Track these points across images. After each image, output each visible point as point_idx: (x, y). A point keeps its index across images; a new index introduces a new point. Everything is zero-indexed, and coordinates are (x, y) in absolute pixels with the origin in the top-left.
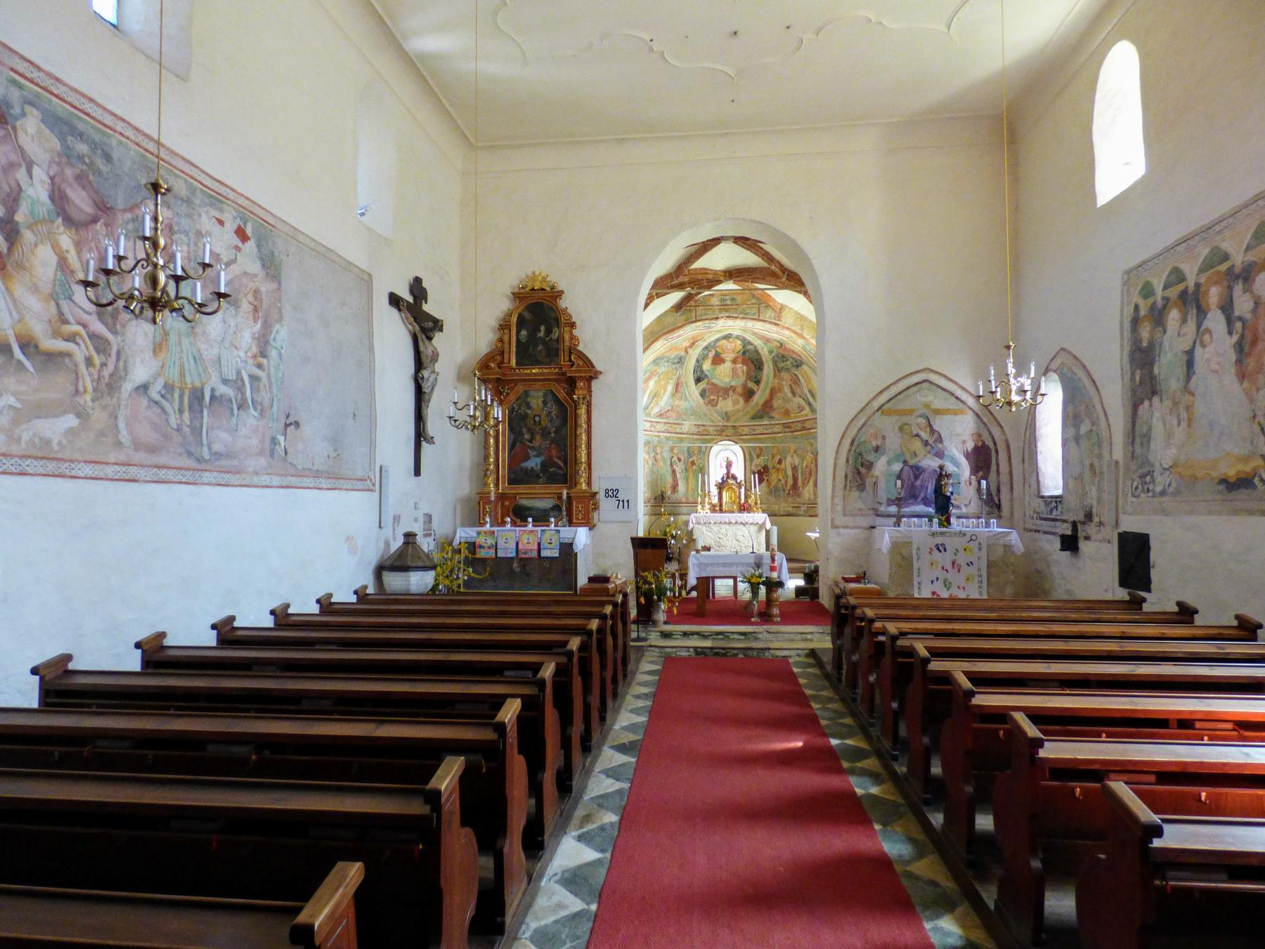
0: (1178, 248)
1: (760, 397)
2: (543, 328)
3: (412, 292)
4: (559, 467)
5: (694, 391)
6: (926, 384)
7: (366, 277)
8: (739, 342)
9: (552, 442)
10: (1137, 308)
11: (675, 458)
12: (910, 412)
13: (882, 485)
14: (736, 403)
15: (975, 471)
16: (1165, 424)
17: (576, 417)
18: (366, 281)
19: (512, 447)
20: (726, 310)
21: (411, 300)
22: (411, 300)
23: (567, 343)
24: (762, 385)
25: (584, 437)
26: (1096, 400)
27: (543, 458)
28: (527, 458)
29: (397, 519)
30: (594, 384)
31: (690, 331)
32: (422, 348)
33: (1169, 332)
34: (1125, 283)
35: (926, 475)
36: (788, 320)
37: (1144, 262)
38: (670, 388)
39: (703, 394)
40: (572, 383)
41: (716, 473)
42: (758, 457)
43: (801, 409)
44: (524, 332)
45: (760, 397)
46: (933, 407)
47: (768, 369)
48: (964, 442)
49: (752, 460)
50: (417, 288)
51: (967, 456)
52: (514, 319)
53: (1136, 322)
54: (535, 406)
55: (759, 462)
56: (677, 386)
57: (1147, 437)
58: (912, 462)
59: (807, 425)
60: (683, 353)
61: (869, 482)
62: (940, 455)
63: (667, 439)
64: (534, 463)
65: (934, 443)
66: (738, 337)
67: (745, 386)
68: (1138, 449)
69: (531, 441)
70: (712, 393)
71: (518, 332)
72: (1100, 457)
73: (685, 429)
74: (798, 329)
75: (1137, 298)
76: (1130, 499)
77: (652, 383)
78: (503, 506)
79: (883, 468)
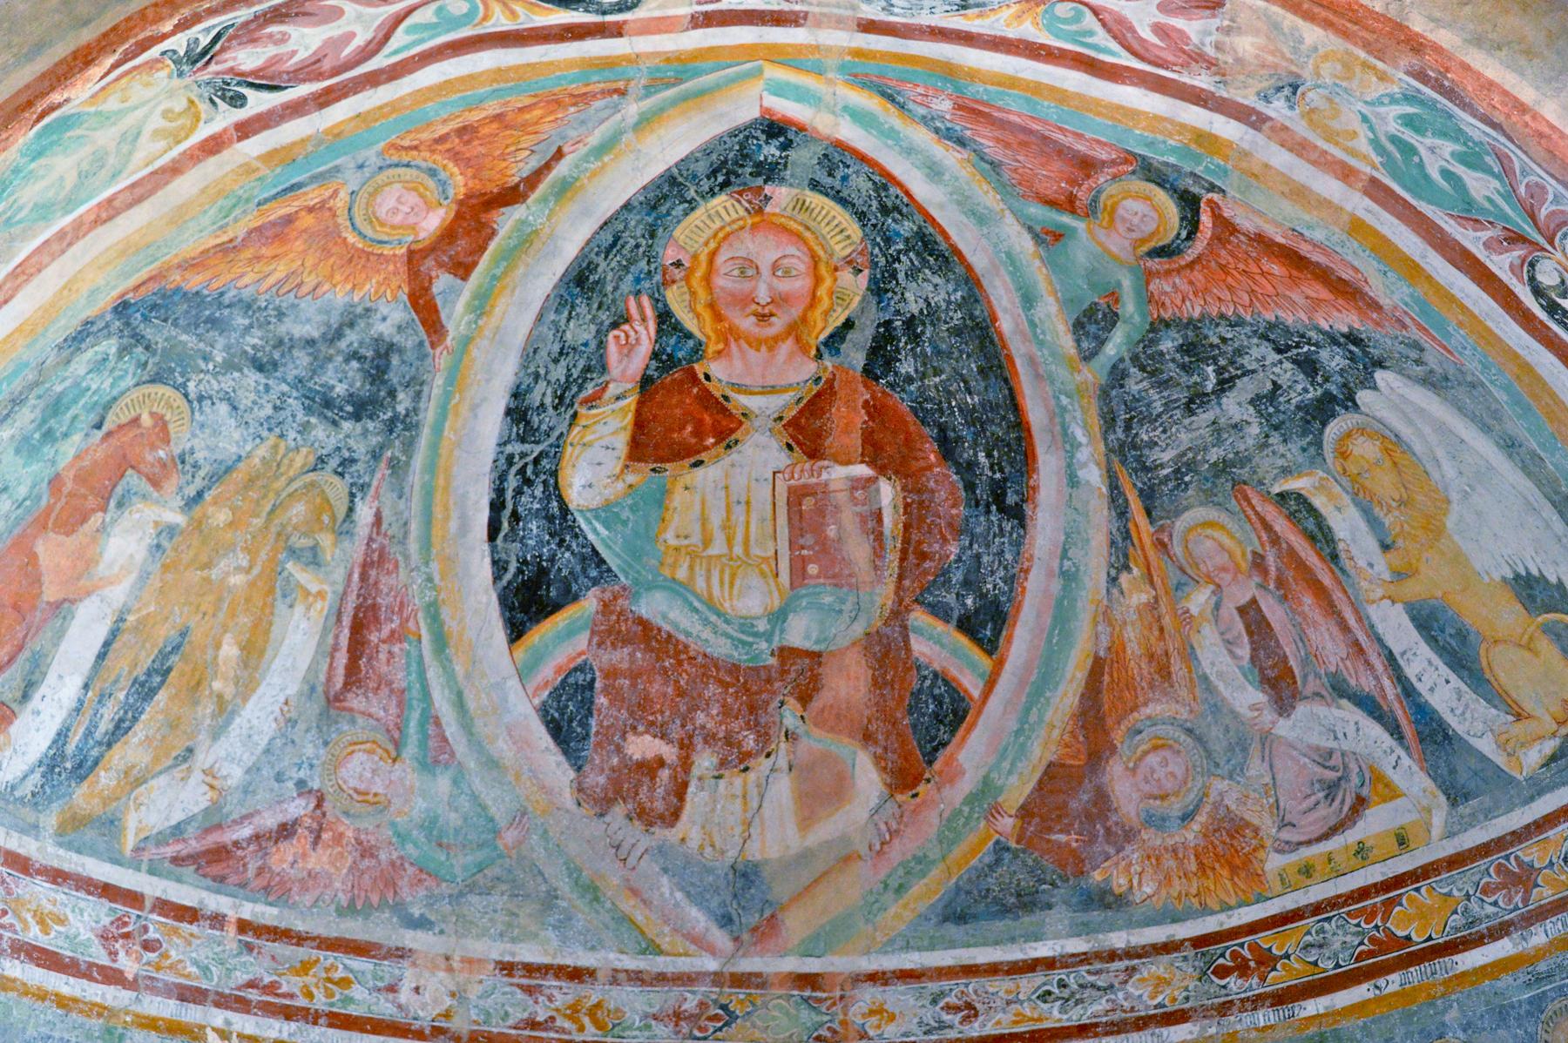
1: (1003, 752)
5: (498, 683)
8: (840, 231)
14: (821, 791)
24: (1021, 641)
38: (301, 641)
39: (566, 721)
43: (1348, 793)
45: (1003, 752)
47: (1070, 483)
59: (1411, 921)
67: (887, 652)
70: (642, 714)
77: (125, 542)
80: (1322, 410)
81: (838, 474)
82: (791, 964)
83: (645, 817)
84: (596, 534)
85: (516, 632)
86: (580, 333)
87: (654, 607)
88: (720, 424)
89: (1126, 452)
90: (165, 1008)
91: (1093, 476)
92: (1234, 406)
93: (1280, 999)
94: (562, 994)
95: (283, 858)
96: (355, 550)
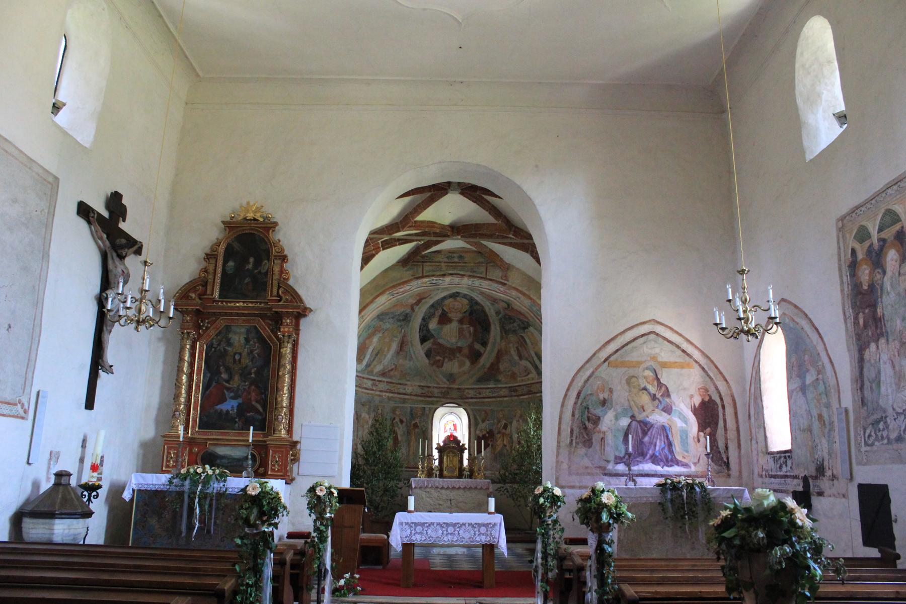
0: (889, 191)
1: (486, 360)
2: (252, 260)
3: (108, 206)
4: (258, 412)
5: (418, 350)
6: (652, 336)
7: (51, 179)
8: (466, 302)
9: (251, 384)
10: (853, 251)
11: (397, 420)
12: (638, 364)
13: (610, 439)
14: (462, 364)
15: (702, 427)
16: (894, 366)
17: (280, 356)
18: (50, 185)
19: (207, 387)
20: (455, 268)
21: (106, 214)
22: (106, 214)
23: (276, 277)
25: (287, 378)
26: (820, 348)
27: (240, 400)
28: (223, 400)
29: (54, 456)
30: (303, 322)
31: (416, 286)
32: (111, 266)
33: (889, 273)
34: (841, 230)
35: (654, 431)
36: (514, 280)
37: (857, 208)
38: (394, 346)
39: (428, 354)
40: (277, 320)
41: (438, 437)
42: (483, 421)
43: (528, 373)
44: (231, 264)
45: (486, 360)
46: (660, 359)
47: (495, 330)
48: (691, 397)
49: (477, 424)
50: (115, 202)
51: (695, 411)
52: (222, 249)
53: (853, 265)
54: (236, 344)
55: (484, 426)
56: (402, 345)
57: (877, 381)
58: (640, 417)
60: (408, 310)
61: (596, 438)
62: (668, 410)
63: (389, 399)
64: (230, 406)
65: (662, 397)
66: (465, 296)
67: (471, 347)
68: (867, 393)
69: (228, 381)
71: (225, 262)
72: (828, 406)
73: (409, 389)
74: (524, 289)
75: (852, 243)
76: (864, 449)
77: (375, 339)
78: (190, 451)
79: (612, 423)
80: (524, 328)
81: (465, 326)
82: (457, 387)
83: (438, 367)
84: (433, 332)
85: (422, 343)
86: (432, 311)
87: (440, 341)
88: (450, 321)
89: (502, 327)
90: (378, 393)
91: (498, 328)
92: (515, 324)
93: (518, 396)
94: (426, 389)
95: (392, 373)
96: (401, 335)
